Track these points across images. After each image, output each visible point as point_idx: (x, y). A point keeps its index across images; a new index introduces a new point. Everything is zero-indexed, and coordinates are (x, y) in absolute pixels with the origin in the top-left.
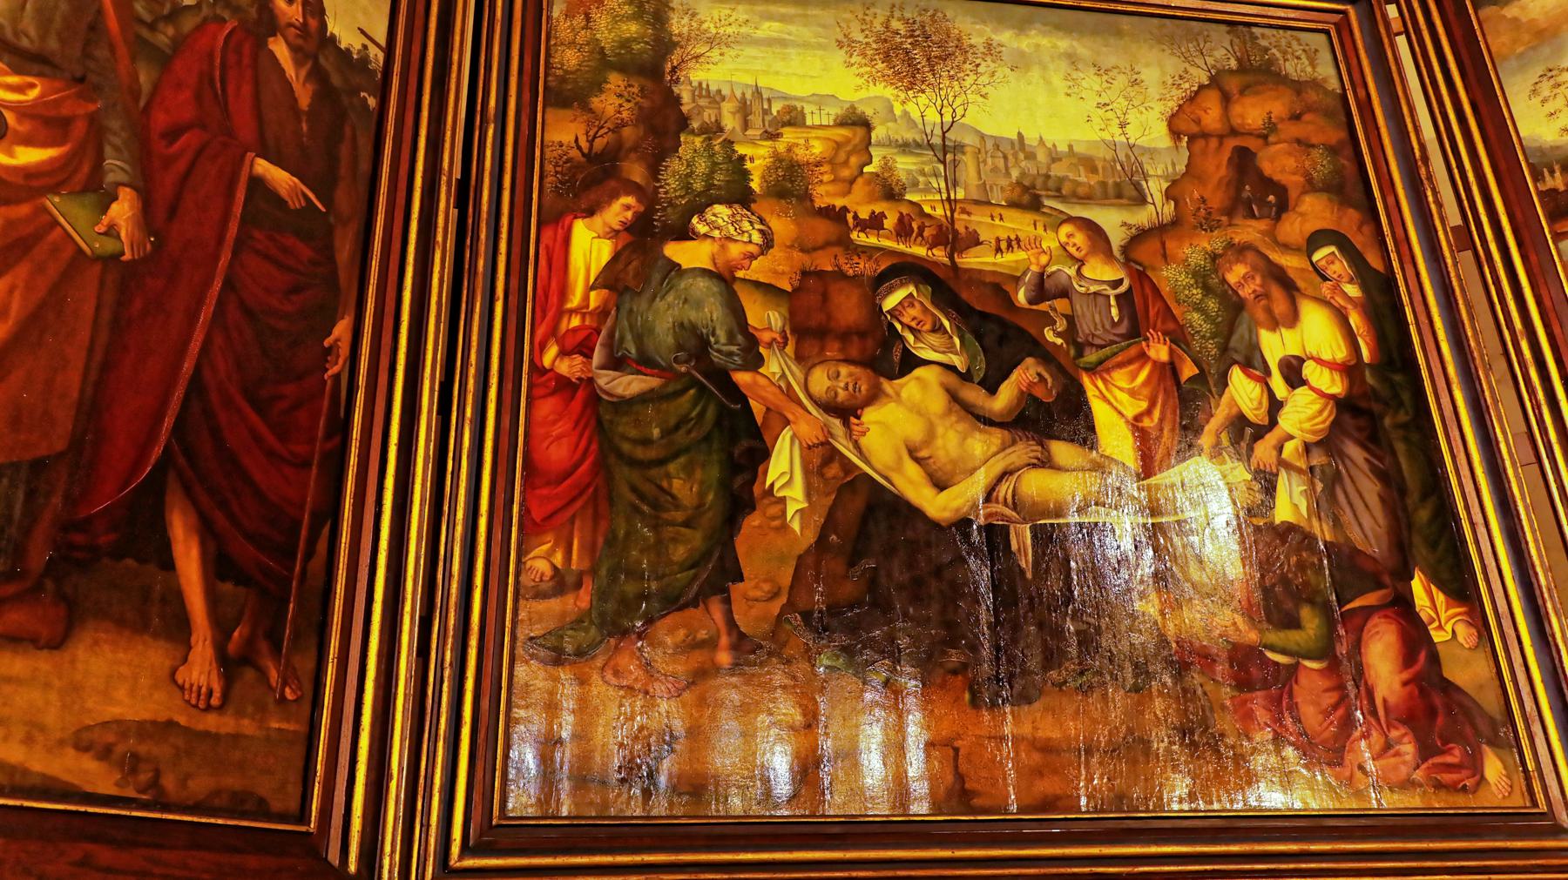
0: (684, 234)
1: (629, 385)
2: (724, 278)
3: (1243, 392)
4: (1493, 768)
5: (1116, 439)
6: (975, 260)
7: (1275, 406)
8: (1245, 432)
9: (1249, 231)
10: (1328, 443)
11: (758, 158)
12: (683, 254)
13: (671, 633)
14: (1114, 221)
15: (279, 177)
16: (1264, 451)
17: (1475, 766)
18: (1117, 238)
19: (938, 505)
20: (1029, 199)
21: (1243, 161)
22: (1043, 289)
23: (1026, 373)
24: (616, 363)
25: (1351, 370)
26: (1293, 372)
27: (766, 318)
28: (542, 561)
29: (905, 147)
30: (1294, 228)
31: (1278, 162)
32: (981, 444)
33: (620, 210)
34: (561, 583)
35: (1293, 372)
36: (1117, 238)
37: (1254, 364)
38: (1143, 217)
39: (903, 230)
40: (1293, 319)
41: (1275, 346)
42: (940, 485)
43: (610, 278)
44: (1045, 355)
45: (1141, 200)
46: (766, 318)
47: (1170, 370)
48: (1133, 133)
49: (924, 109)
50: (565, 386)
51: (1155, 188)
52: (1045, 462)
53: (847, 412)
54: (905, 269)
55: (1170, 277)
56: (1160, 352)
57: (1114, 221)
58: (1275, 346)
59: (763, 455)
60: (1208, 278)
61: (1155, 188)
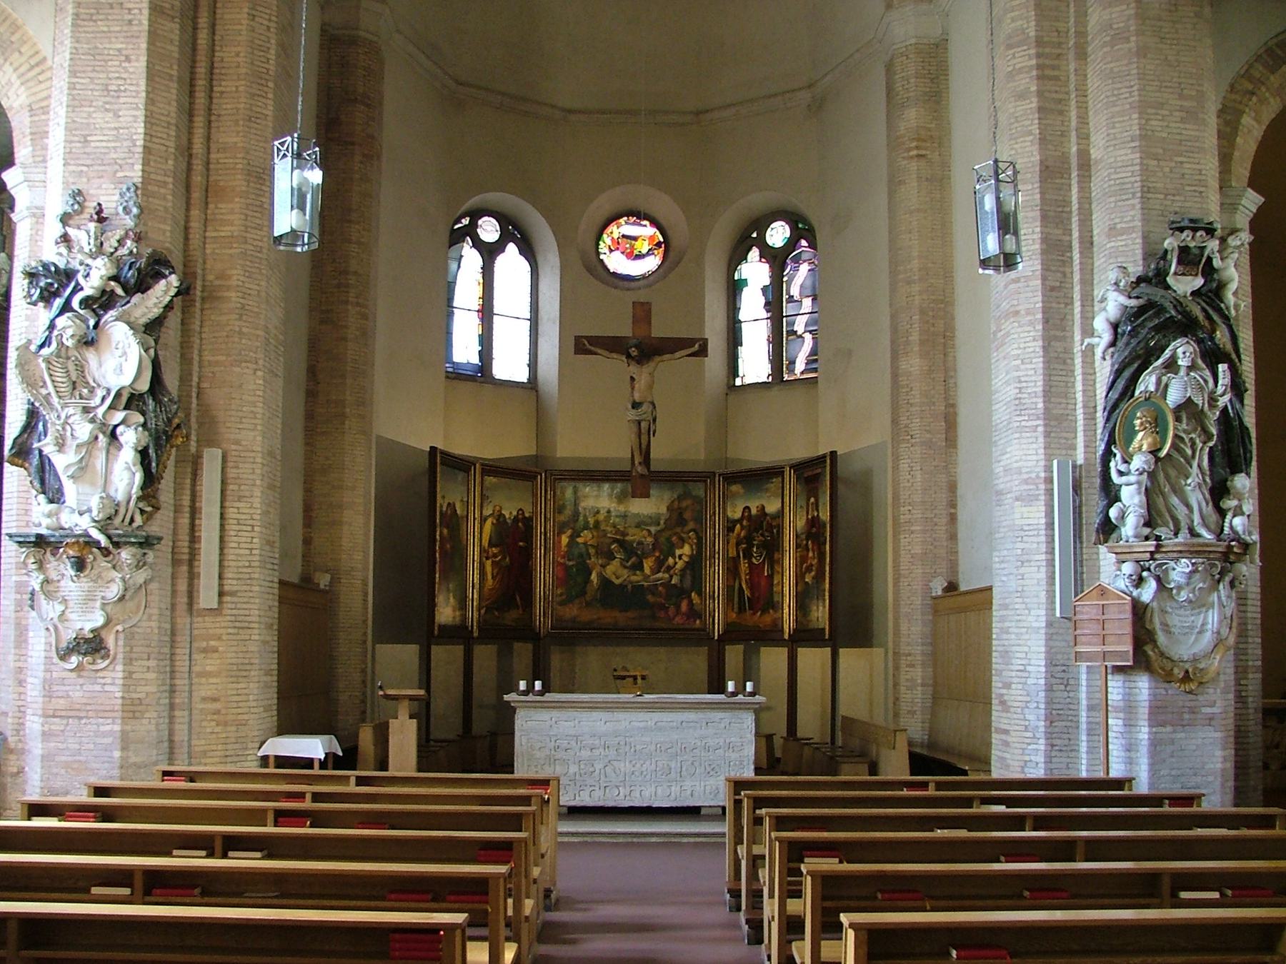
0: (580, 536)
1: (571, 563)
2: (585, 544)
3: (671, 560)
4: (698, 622)
5: (647, 571)
6: (628, 538)
7: (676, 563)
8: (669, 568)
9: (678, 530)
10: (683, 570)
11: (591, 520)
12: (580, 540)
13: (577, 601)
14: (653, 529)
15: (521, 544)
16: (672, 572)
17: (695, 621)
18: (653, 532)
19: (617, 582)
20: (638, 526)
21: (681, 514)
22: (640, 543)
23: (633, 559)
24: (569, 560)
25: (691, 557)
26: (680, 557)
27: (592, 551)
28: (559, 592)
29: (617, 516)
30: (686, 529)
31: (687, 515)
32: (626, 571)
33: (569, 532)
34: (561, 595)
35: (680, 557)
36: (653, 532)
37: (674, 557)
38: (659, 528)
39: (616, 534)
40: (682, 547)
41: (678, 552)
42: (617, 578)
43: (569, 545)
44: (637, 555)
45: (659, 524)
46: (592, 551)
47: (658, 557)
48: (661, 512)
49: (622, 508)
50: (561, 564)
51: (662, 522)
52: (635, 574)
53: (603, 566)
54: (616, 541)
55: (662, 540)
56: (657, 554)
57: (653, 529)
58: (678, 552)
59: (591, 574)
60: (668, 540)
61: (662, 522)
